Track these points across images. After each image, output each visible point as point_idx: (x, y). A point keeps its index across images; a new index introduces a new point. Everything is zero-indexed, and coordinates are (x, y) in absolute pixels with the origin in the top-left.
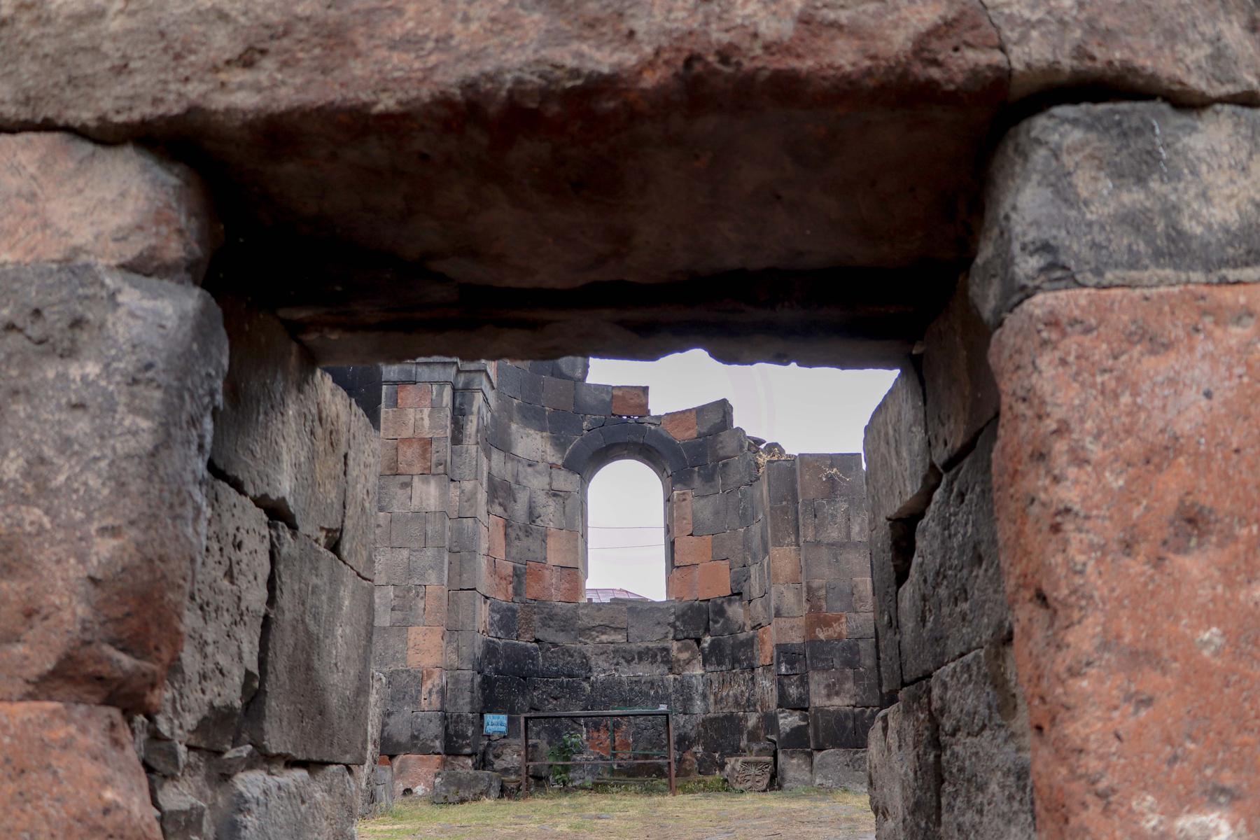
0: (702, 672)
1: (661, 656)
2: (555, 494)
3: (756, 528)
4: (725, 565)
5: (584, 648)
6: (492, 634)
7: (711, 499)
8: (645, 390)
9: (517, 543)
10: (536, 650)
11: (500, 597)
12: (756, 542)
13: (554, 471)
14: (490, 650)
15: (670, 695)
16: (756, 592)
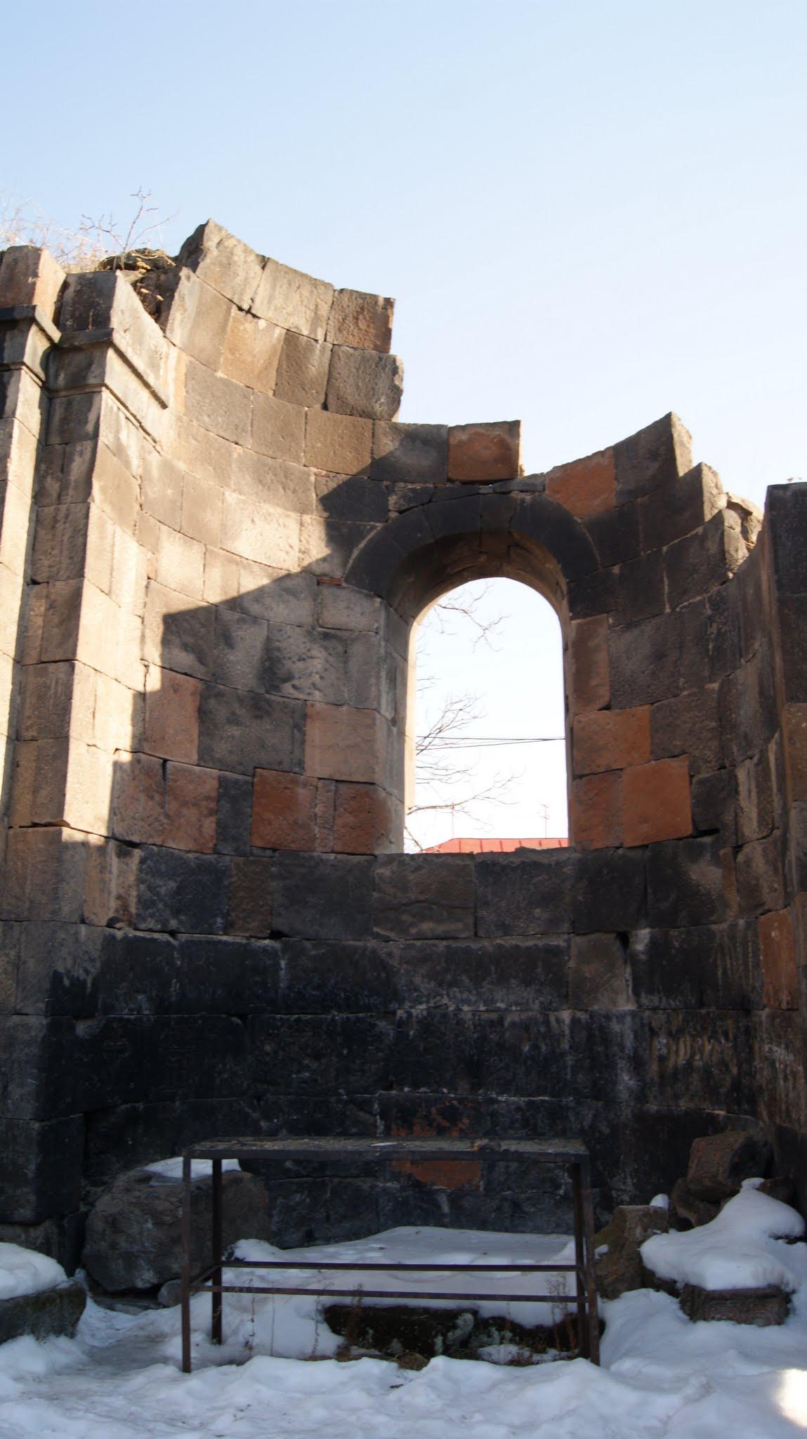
0: (631, 1007)
1: (544, 969)
2: (329, 636)
3: (747, 675)
4: (679, 767)
5: (383, 949)
6: (151, 923)
7: (648, 628)
8: (513, 427)
9: (235, 731)
10: (274, 954)
11: (179, 844)
12: (747, 710)
13: (327, 591)
14: (128, 959)
15: (563, 1054)
16: (751, 825)
